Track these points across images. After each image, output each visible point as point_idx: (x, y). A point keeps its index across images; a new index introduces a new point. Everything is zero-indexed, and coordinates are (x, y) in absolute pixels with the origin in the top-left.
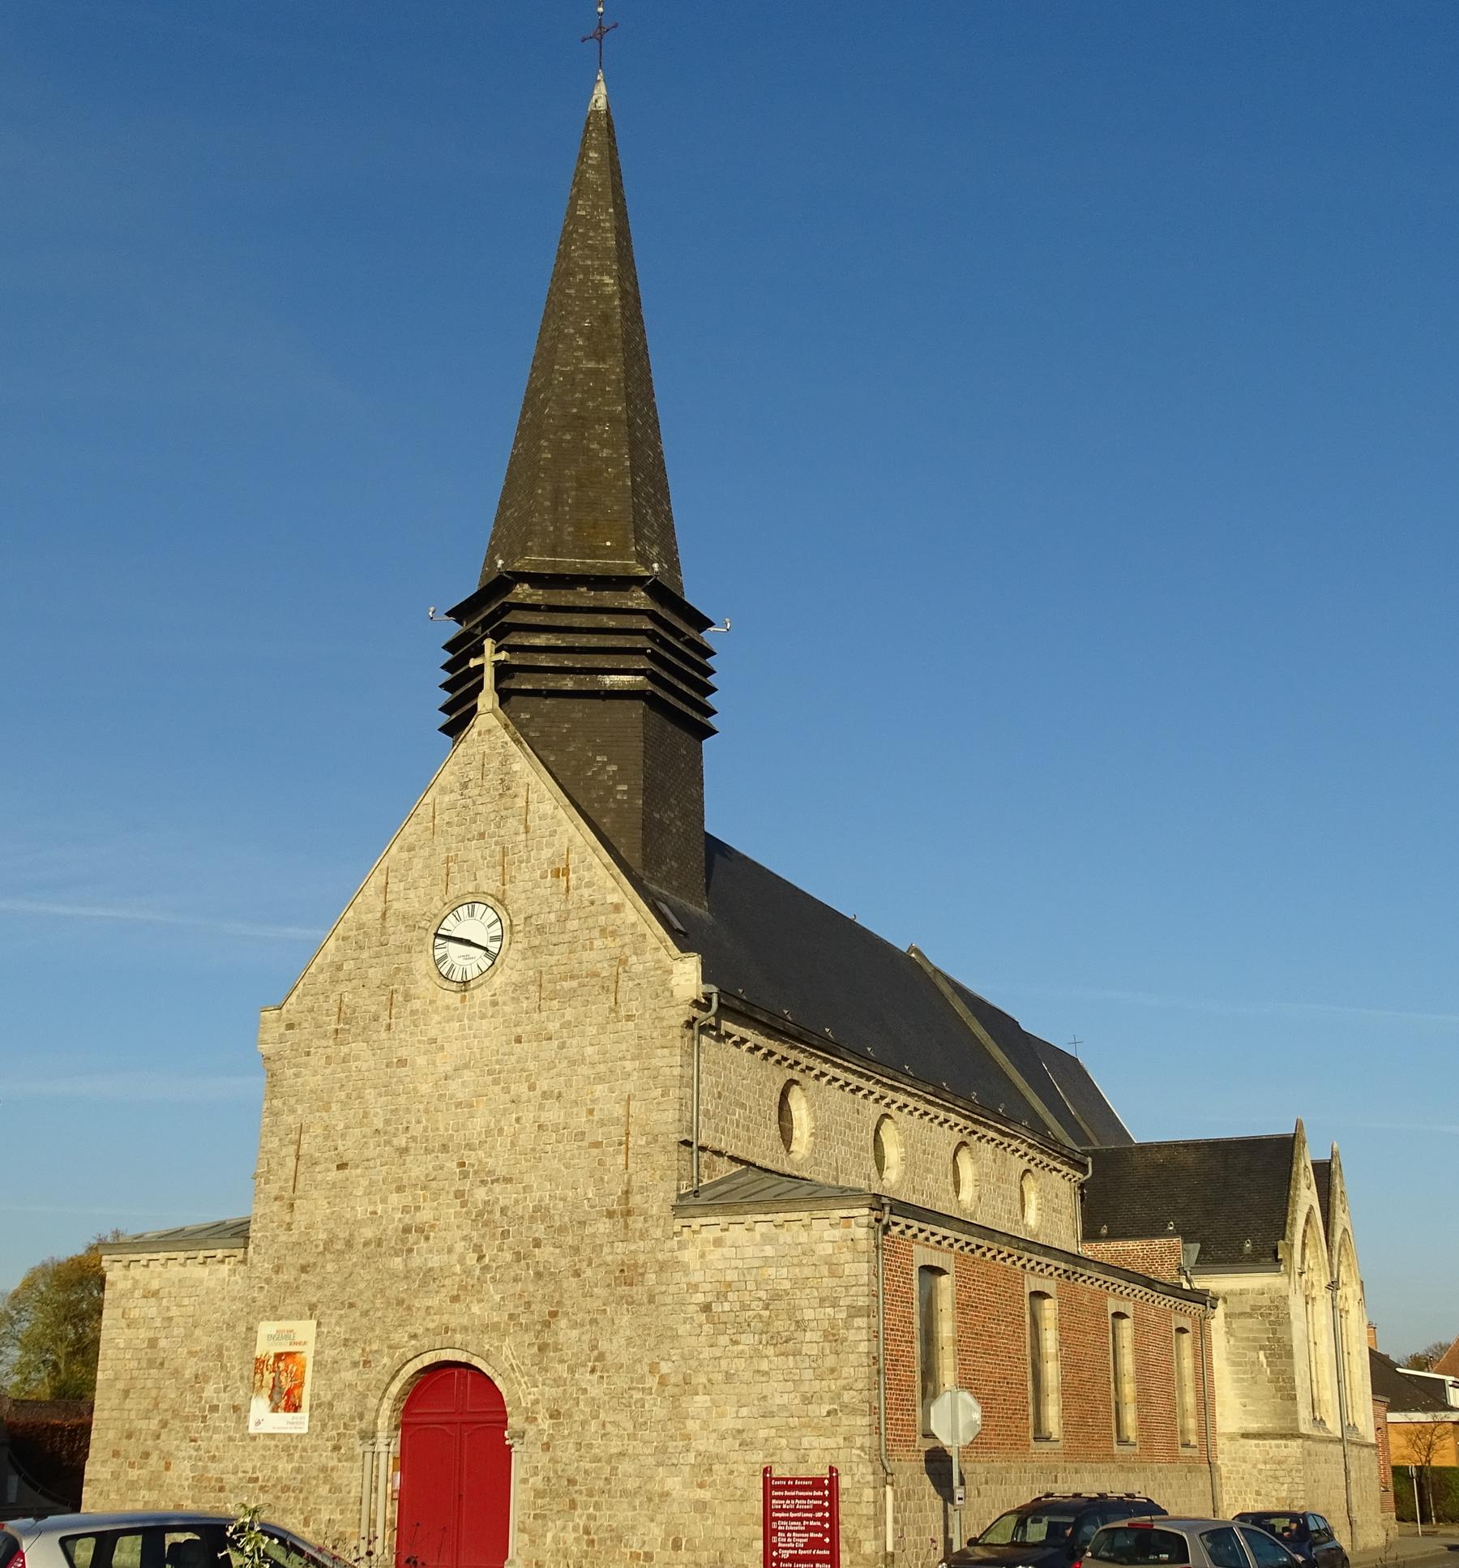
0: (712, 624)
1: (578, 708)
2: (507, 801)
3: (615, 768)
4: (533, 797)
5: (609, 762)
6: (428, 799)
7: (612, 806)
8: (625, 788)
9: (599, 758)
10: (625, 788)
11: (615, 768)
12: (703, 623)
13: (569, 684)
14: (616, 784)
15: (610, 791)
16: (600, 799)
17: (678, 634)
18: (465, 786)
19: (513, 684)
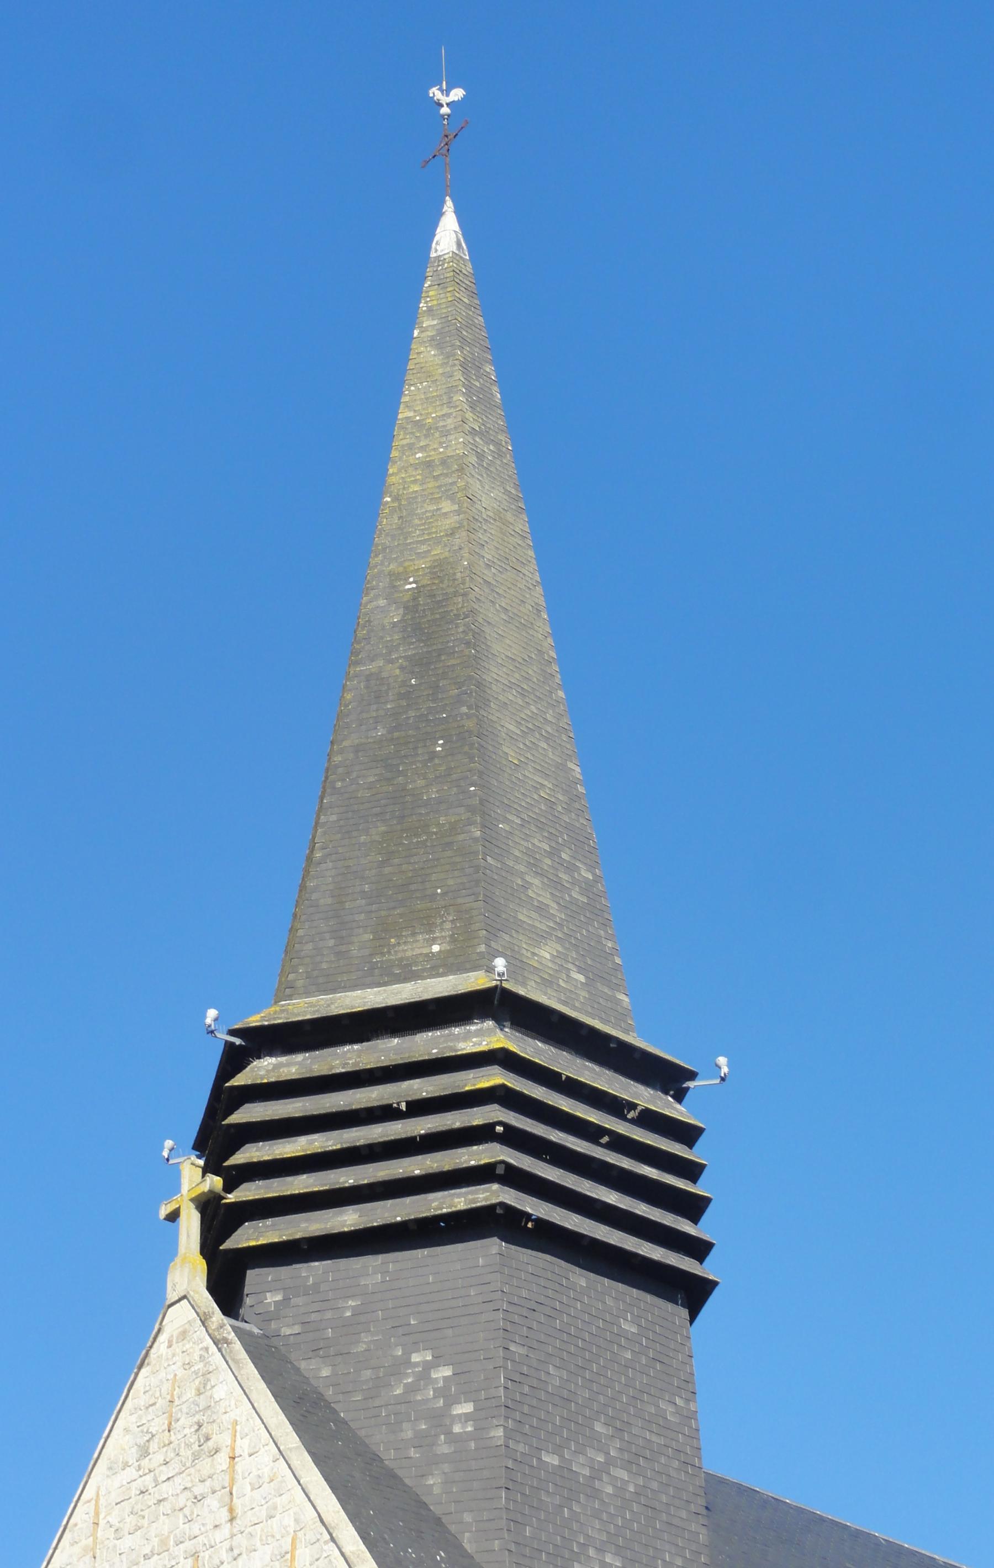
0: (692, 1075)
1: (371, 1269)
2: (205, 1465)
3: (447, 1372)
4: (243, 1446)
5: (438, 1360)
6: (89, 1493)
7: (444, 1448)
8: (467, 1408)
9: (416, 1358)
10: (467, 1408)
11: (447, 1372)
12: (671, 1078)
13: (348, 1219)
14: (452, 1401)
15: (440, 1419)
16: (424, 1442)
17: (615, 1106)
18: (144, 1452)
19: (250, 1235)
